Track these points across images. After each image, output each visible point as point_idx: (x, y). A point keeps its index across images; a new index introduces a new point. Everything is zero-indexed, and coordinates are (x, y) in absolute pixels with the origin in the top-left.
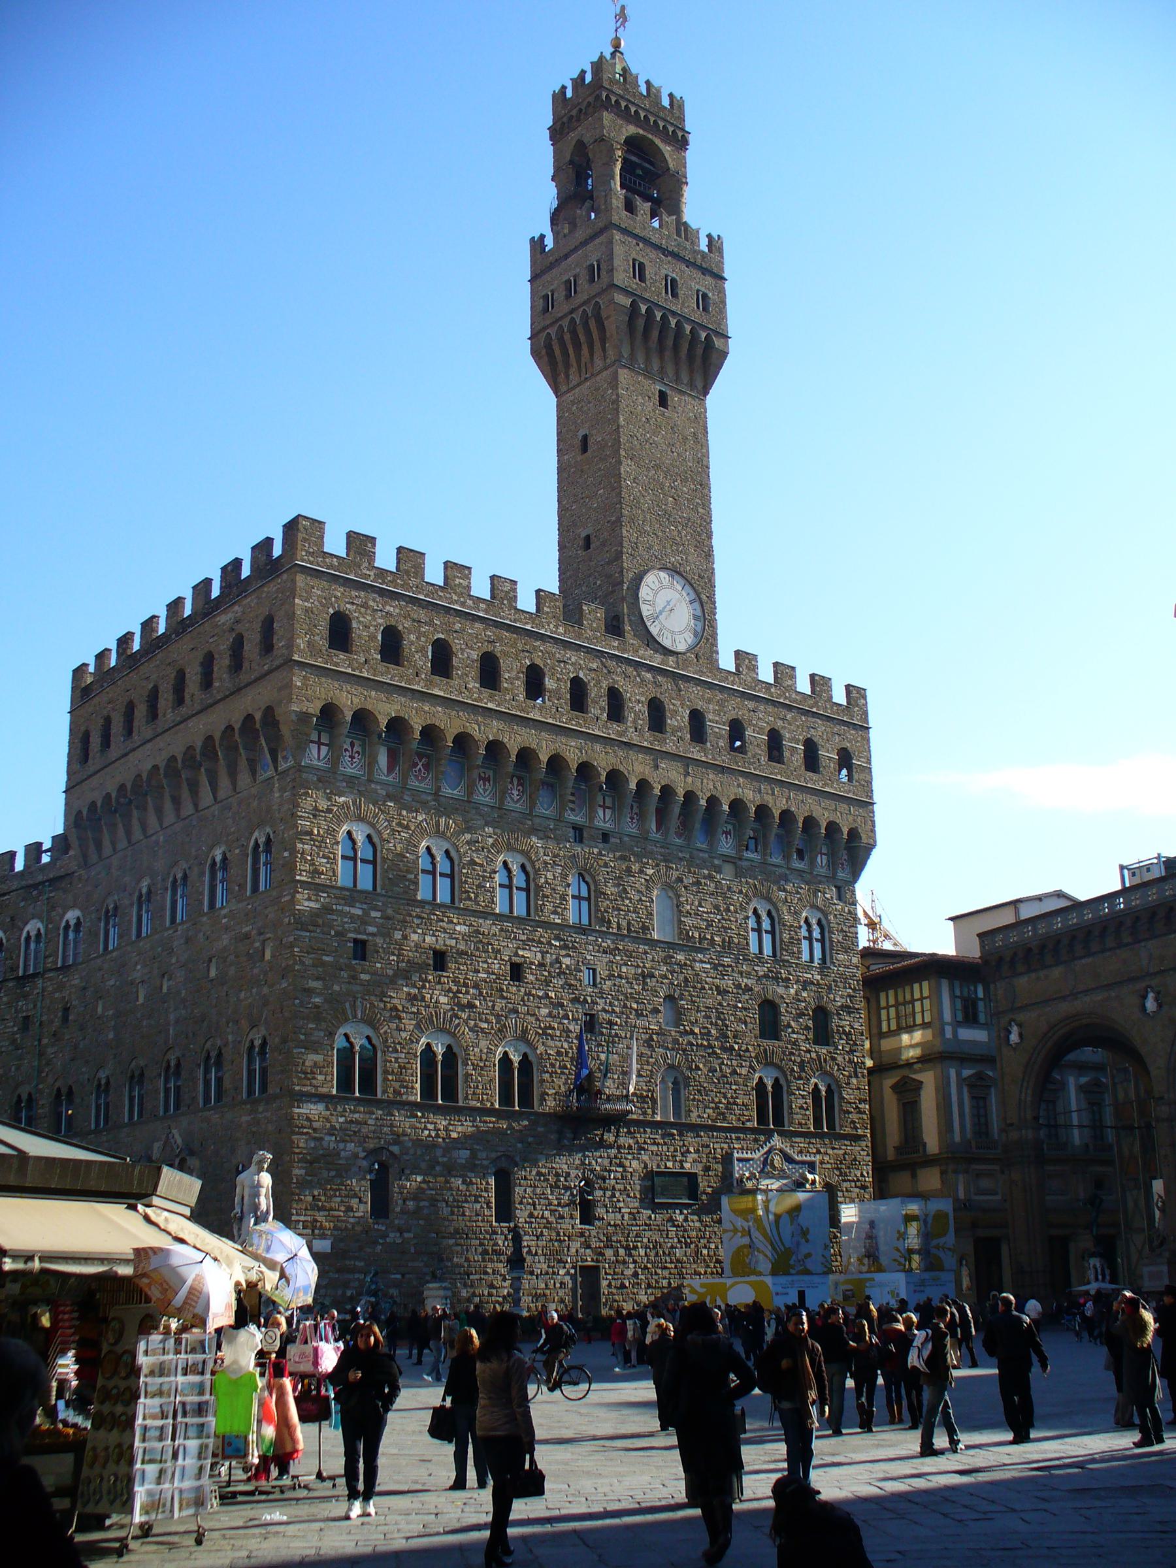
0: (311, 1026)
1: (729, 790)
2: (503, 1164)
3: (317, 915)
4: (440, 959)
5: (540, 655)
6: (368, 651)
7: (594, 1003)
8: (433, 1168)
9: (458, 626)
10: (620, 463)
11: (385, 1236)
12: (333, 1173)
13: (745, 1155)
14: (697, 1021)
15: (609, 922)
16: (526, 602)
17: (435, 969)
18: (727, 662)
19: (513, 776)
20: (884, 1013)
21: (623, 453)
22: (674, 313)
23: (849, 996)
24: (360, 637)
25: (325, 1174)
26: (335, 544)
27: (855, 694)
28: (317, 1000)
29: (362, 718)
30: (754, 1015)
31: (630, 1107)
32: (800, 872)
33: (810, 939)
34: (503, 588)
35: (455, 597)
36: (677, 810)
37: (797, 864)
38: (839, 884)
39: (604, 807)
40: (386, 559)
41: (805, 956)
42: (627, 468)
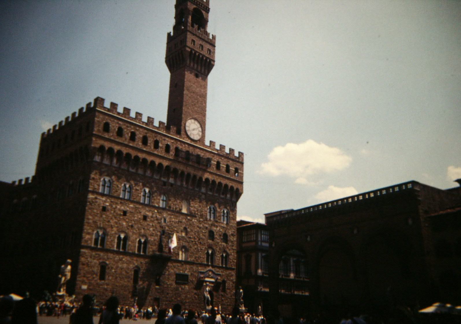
4: (125, 213)
5: (158, 138)
7: (165, 228)
10: (183, 90)
14: (192, 234)
15: (170, 207)
16: (156, 124)
18: (207, 143)
20: (244, 237)
21: (185, 88)
22: (201, 54)
24: (112, 129)
26: (107, 105)
27: (241, 154)
28: (91, 221)
30: (207, 234)
31: (172, 255)
33: (224, 216)
34: (150, 120)
35: (138, 121)
37: (222, 196)
40: (120, 110)
41: (222, 221)
42: (185, 92)
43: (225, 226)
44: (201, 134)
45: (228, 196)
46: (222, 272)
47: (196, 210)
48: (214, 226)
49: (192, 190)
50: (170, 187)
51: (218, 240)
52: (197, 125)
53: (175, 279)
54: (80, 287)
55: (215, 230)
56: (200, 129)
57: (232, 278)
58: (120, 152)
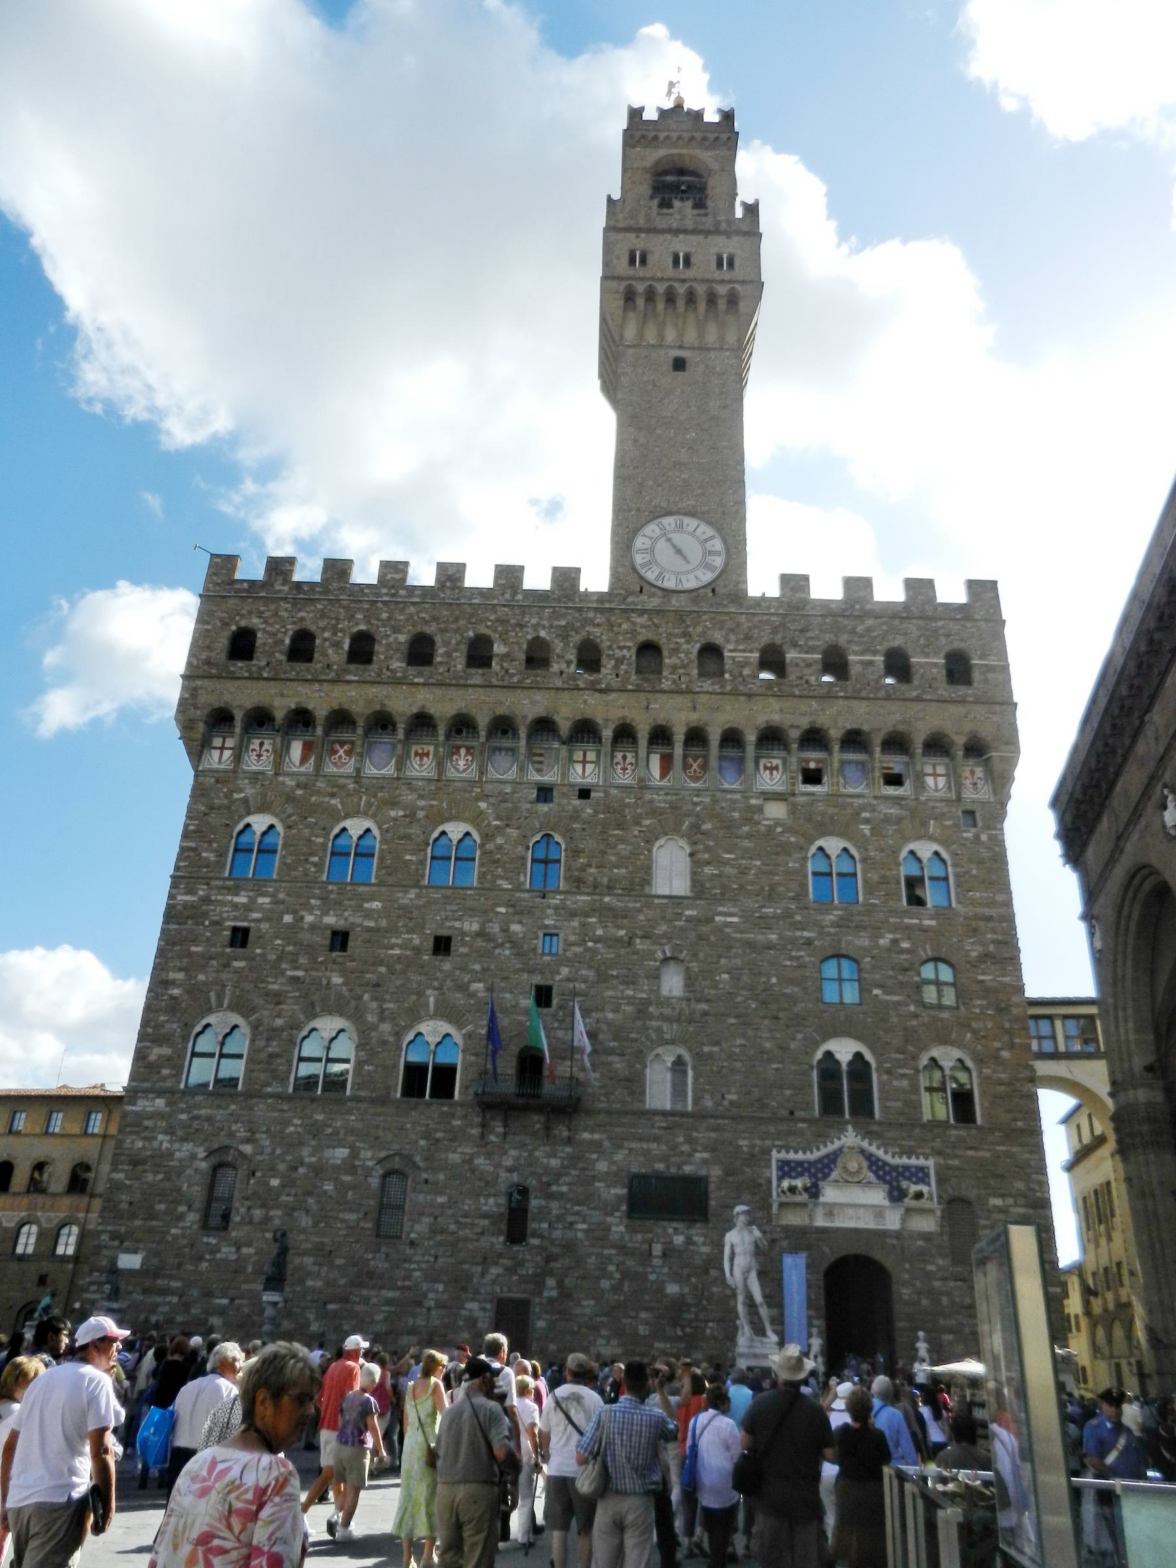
0: (162, 1018)
1: (751, 717)
2: (397, 1163)
3: (193, 907)
4: (340, 939)
6: (272, 654)
7: (558, 973)
8: (295, 1169)
9: (385, 616)
11: (215, 1250)
12: (160, 1176)
13: (792, 1156)
17: (332, 949)
19: (458, 748)
22: (683, 281)
23: (993, 941)
25: (150, 1177)
28: (176, 992)
29: (260, 719)
32: (897, 800)
35: (384, 591)
36: (678, 750)
37: (891, 791)
38: (969, 807)
39: (584, 762)
43: (933, 923)
44: (719, 562)
45: (936, 782)
46: (939, 1153)
47: (729, 870)
48: (860, 927)
49: (698, 792)
50: (577, 802)
51: (895, 994)
52: (693, 534)
53: (624, 1208)
54: (114, 1261)
55: (866, 951)
56: (718, 545)
57: (1020, 1185)
58: (301, 719)
